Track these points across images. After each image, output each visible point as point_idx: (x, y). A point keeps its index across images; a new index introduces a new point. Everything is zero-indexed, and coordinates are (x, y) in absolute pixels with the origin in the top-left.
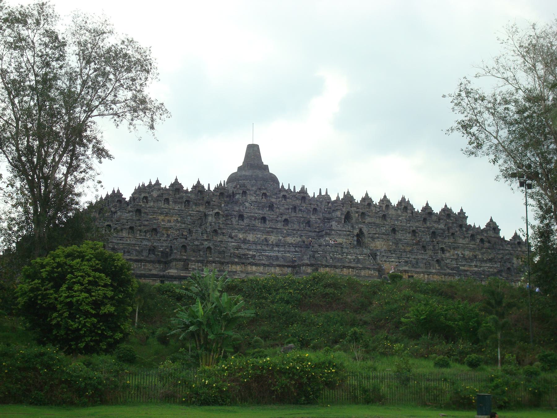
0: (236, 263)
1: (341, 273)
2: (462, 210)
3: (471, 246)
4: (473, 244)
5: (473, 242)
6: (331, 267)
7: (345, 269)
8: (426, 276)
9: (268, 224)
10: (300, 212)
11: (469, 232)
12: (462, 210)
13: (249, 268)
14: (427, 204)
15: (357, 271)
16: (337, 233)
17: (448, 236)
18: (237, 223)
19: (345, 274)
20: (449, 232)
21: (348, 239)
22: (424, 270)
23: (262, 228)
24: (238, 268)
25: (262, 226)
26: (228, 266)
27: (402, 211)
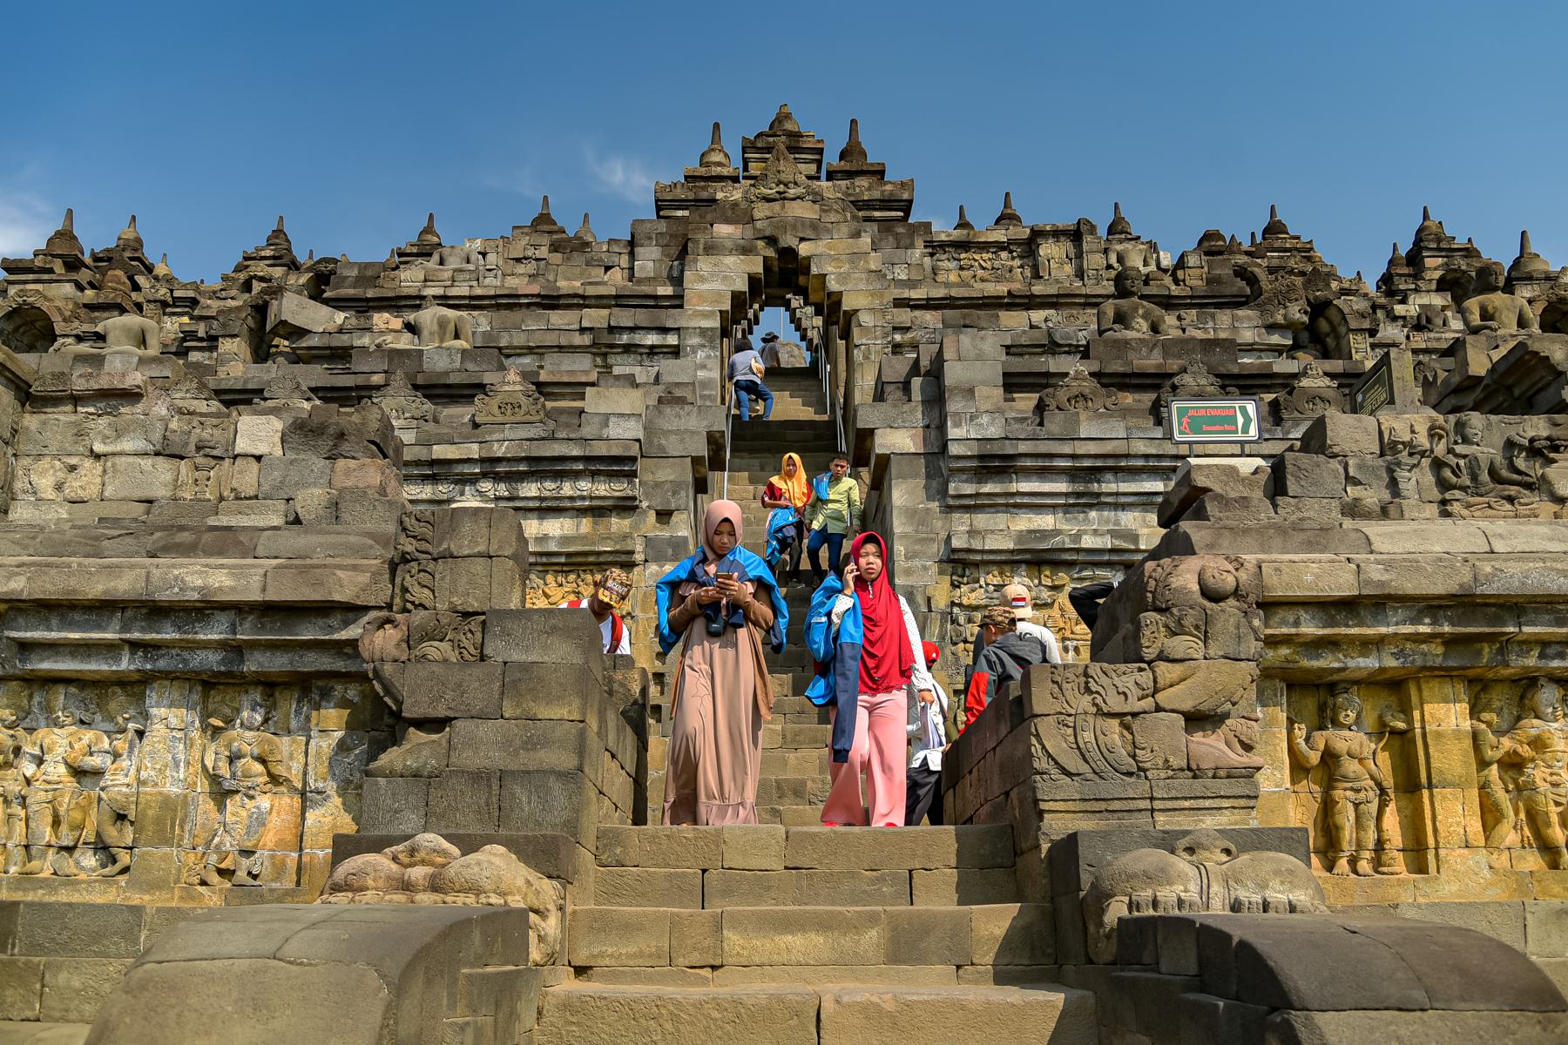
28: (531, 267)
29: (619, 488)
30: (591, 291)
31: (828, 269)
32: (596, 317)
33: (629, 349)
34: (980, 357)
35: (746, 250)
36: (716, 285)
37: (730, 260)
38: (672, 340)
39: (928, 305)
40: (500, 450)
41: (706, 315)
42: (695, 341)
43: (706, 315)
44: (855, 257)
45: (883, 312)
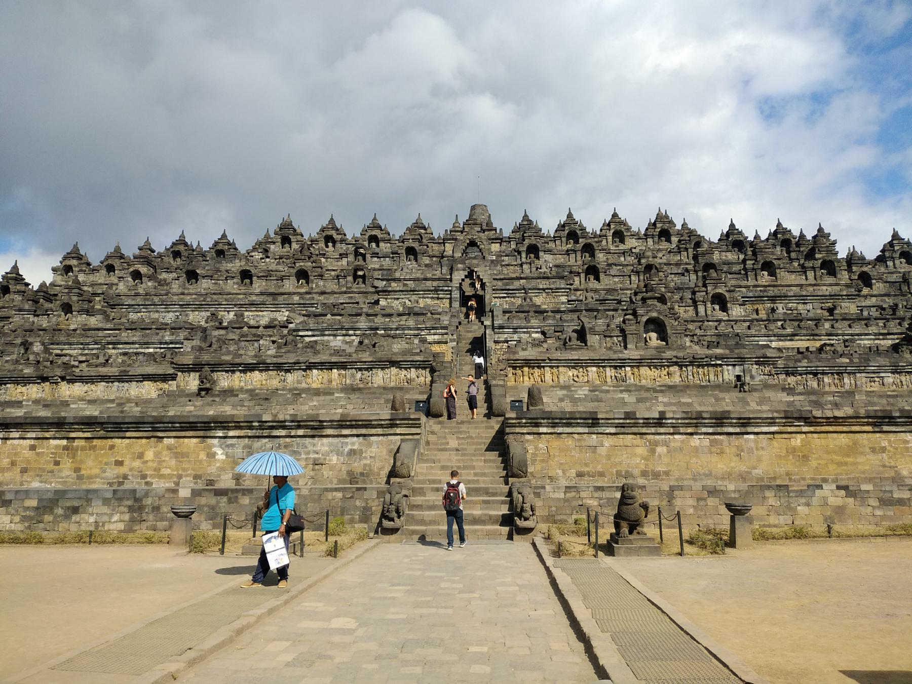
0: (25, 381)
1: (304, 385)
2: (820, 230)
3: (824, 288)
4: (831, 285)
5: (830, 280)
6: (267, 369)
7: (315, 372)
8: (610, 372)
9: (258, 285)
10: (375, 259)
11: (817, 256)
12: (820, 230)
13: (66, 390)
14: (732, 226)
15: (359, 375)
16: (405, 285)
17: (753, 269)
18: (180, 291)
19: (314, 386)
20: (756, 260)
21: (438, 298)
22: (602, 353)
23: (241, 296)
24: (34, 391)
25: (243, 291)
26: (6, 390)
27: (656, 239)
28: (421, 272)
29: (446, 331)
30: (434, 277)
31: (480, 274)
32: (435, 284)
33: (441, 290)
34: (499, 310)
35: (464, 270)
36: (458, 277)
37: (461, 272)
38: (450, 288)
39: (501, 279)
40: (428, 326)
41: (456, 284)
42: (454, 289)
43: (456, 284)
44: (486, 271)
45: (491, 282)
